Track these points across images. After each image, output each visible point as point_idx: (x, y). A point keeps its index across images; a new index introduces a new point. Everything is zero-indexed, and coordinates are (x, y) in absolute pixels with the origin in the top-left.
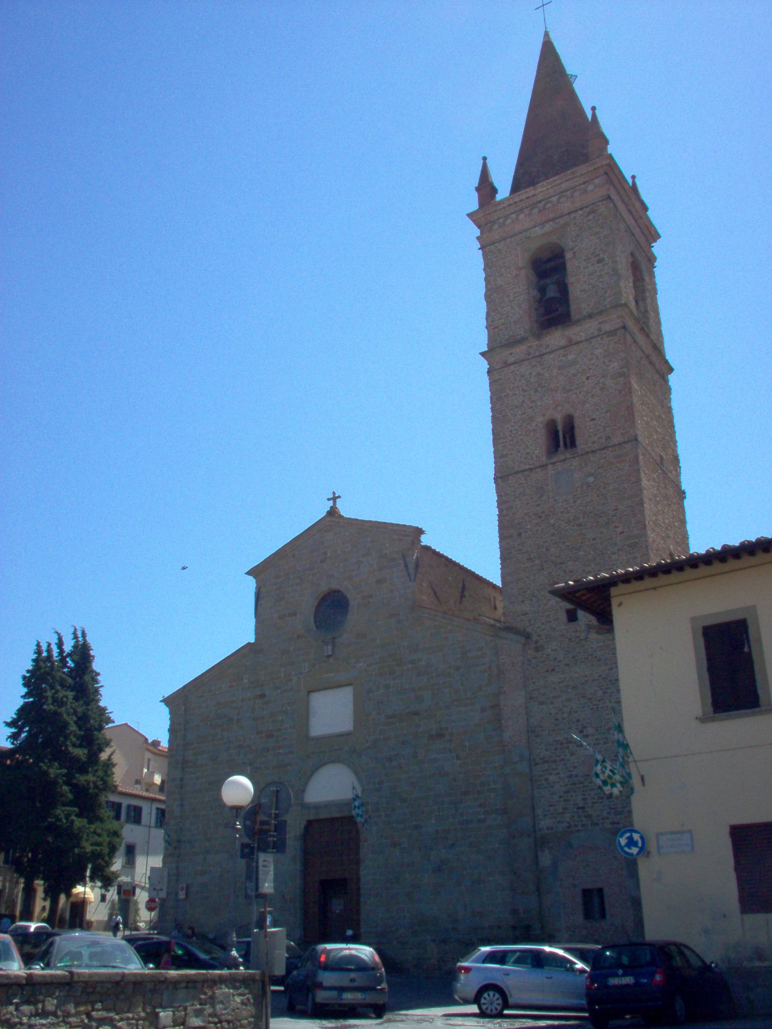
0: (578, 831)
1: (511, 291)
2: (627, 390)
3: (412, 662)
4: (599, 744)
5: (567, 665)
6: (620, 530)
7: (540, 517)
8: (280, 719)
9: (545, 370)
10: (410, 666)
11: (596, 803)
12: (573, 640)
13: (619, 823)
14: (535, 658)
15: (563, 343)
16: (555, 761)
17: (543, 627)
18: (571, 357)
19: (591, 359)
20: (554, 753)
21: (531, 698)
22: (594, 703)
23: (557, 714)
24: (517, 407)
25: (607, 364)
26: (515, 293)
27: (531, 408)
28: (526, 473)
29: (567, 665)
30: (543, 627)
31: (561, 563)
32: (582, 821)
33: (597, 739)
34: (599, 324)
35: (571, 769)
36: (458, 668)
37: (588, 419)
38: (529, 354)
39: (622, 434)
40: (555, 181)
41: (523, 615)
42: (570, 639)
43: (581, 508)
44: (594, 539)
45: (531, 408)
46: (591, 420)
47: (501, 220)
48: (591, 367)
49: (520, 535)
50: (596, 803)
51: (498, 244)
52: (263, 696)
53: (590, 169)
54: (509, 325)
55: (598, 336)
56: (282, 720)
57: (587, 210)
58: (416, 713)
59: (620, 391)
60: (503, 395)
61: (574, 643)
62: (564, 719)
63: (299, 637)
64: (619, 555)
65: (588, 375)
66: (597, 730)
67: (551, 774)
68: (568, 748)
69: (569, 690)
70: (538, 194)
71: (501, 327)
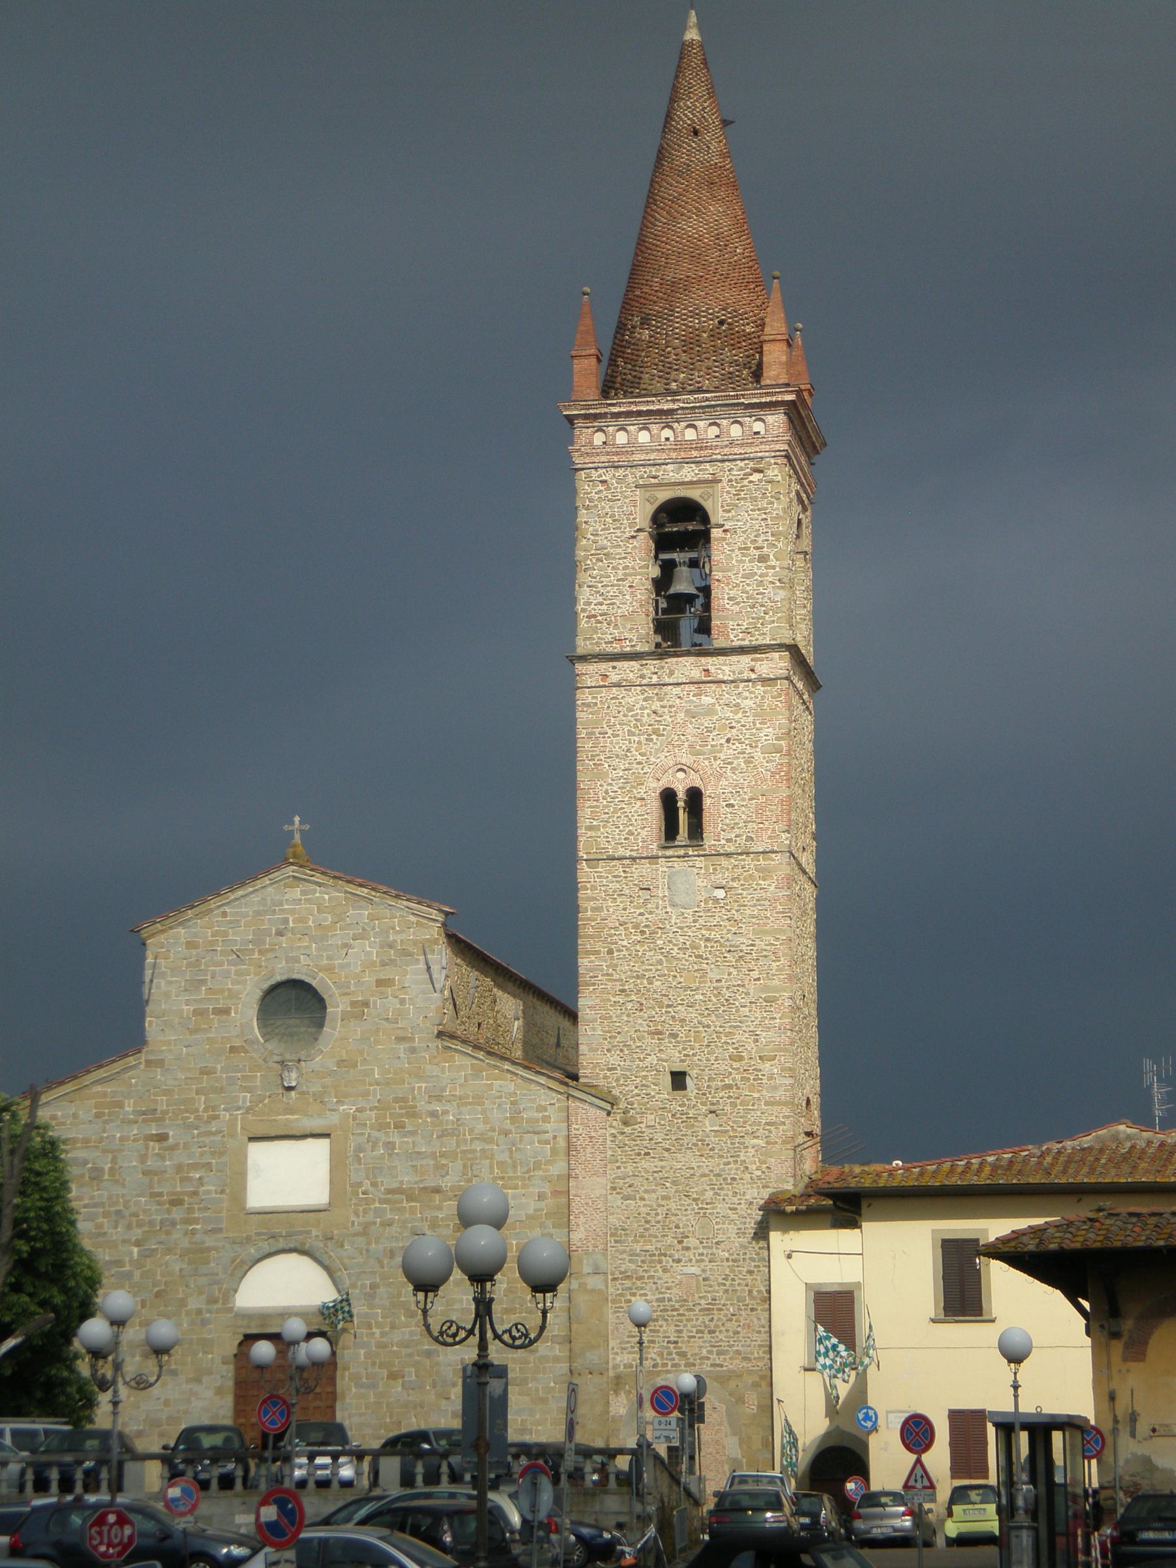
0: (668, 1372)
1: (621, 561)
2: (783, 774)
3: (433, 1114)
4: (703, 1261)
5: (668, 1150)
6: (755, 974)
7: (643, 932)
8: (198, 1176)
9: (666, 710)
10: (429, 1120)
11: (694, 1337)
12: (678, 1116)
13: (721, 1366)
14: (623, 1133)
15: (696, 674)
16: (642, 1278)
17: (636, 1091)
18: (707, 700)
19: (736, 713)
20: (641, 1267)
21: (614, 1189)
22: (700, 1206)
23: (648, 1214)
24: (617, 756)
25: (758, 725)
26: (626, 568)
27: (639, 763)
28: (624, 862)
29: (668, 1150)
30: (636, 1091)
31: (669, 1006)
32: (673, 1359)
33: (702, 1254)
34: (752, 660)
35: (663, 1290)
36: (506, 1133)
37: (725, 803)
38: (642, 677)
39: (770, 838)
40: (707, 400)
41: (609, 1069)
42: (673, 1115)
43: (704, 932)
44: (719, 981)
45: (639, 763)
46: (726, 805)
47: (610, 428)
48: (734, 724)
49: (610, 952)
50: (694, 1337)
51: (604, 470)
52: (162, 1138)
53: (763, 400)
54: (613, 618)
55: (749, 681)
56: (200, 1178)
57: (751, 465)
58: (437, 1190)
59: (773, 774)
60: (597, 731)
61: (680, 1121)
62: (658, 1222)
63: (233, 1049)
64: (750, 1011)
65: (729, 735)
66: (701, 1243)
67: (634, 1295)
68: (660, 1262)
69: (668, 1185)
70: (677, 409)
71: (599, 618)
